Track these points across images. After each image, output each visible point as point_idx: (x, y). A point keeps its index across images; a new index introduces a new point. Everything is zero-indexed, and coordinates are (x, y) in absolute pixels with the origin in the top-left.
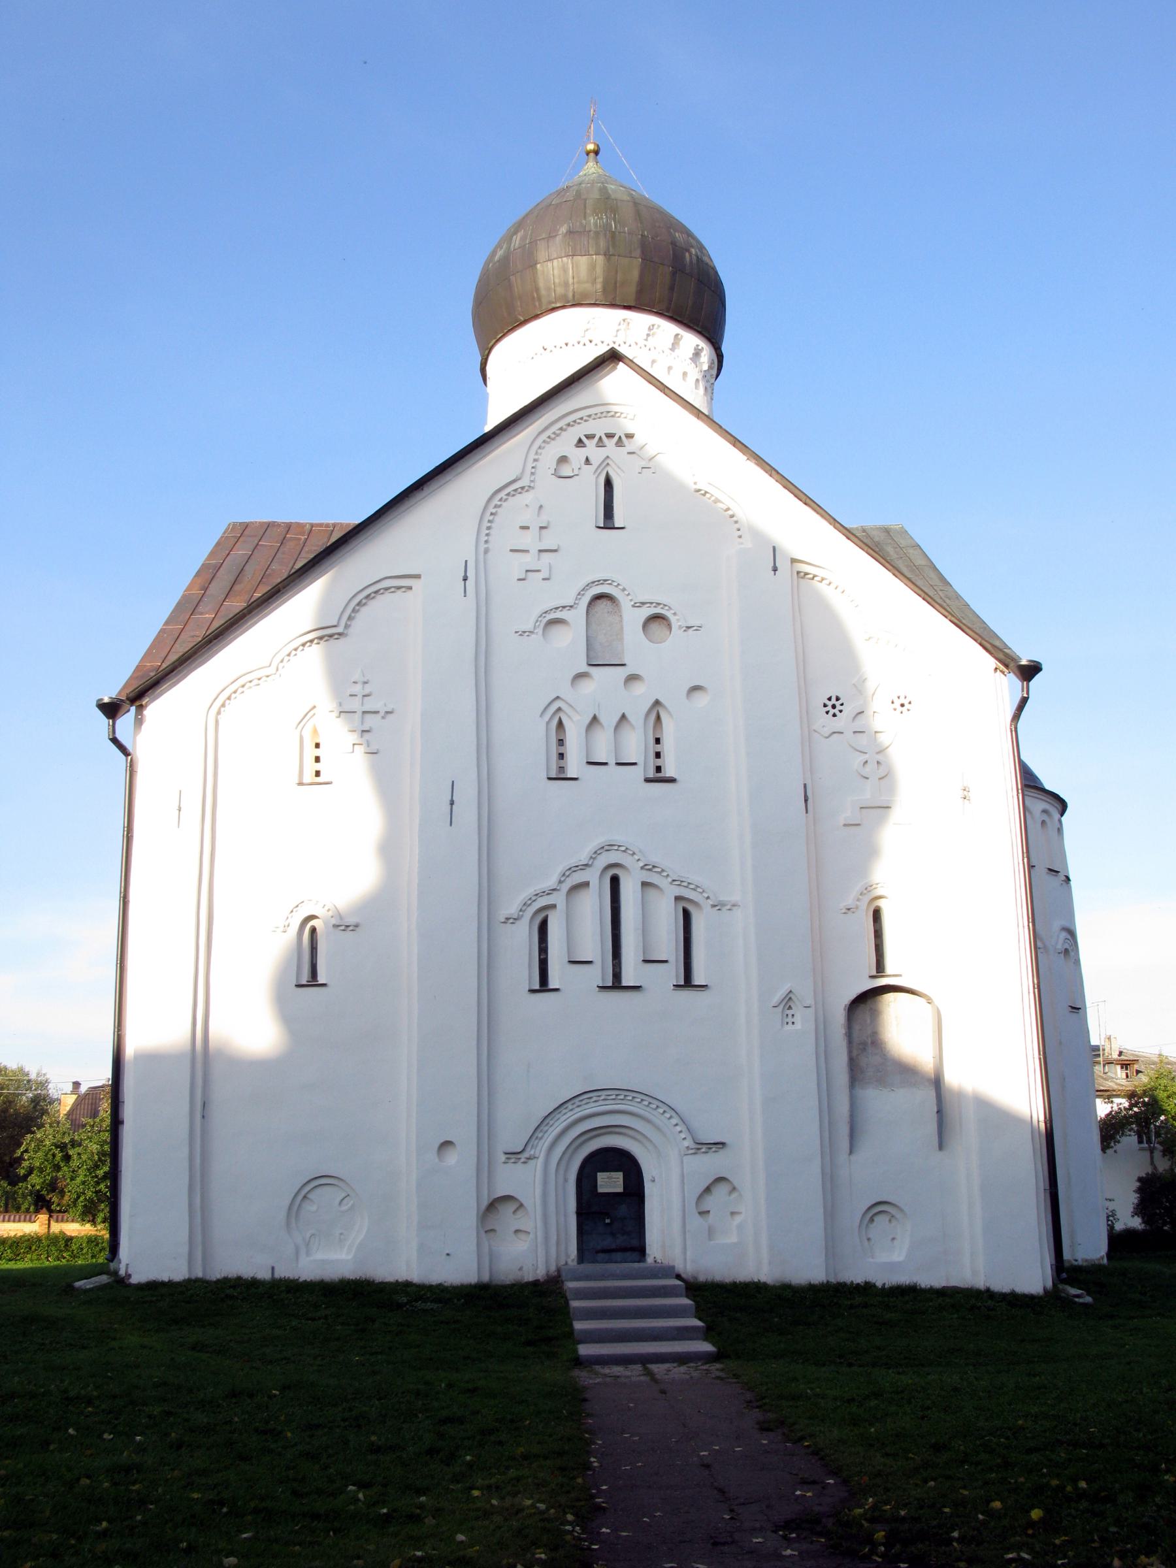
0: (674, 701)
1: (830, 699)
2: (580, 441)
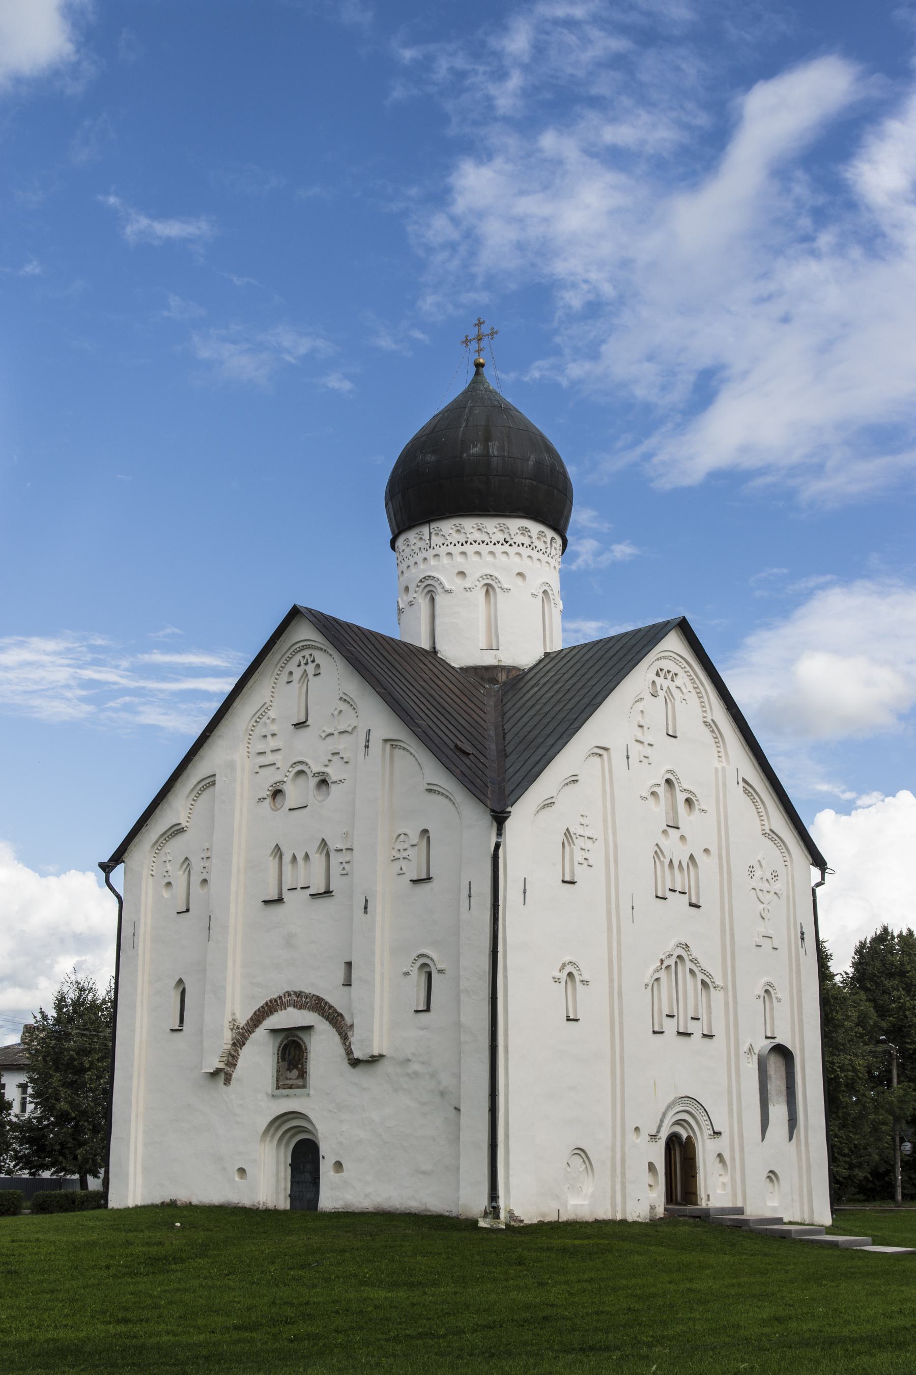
0: (700, 857)
1: (750, 867)
2: (658, 671)
